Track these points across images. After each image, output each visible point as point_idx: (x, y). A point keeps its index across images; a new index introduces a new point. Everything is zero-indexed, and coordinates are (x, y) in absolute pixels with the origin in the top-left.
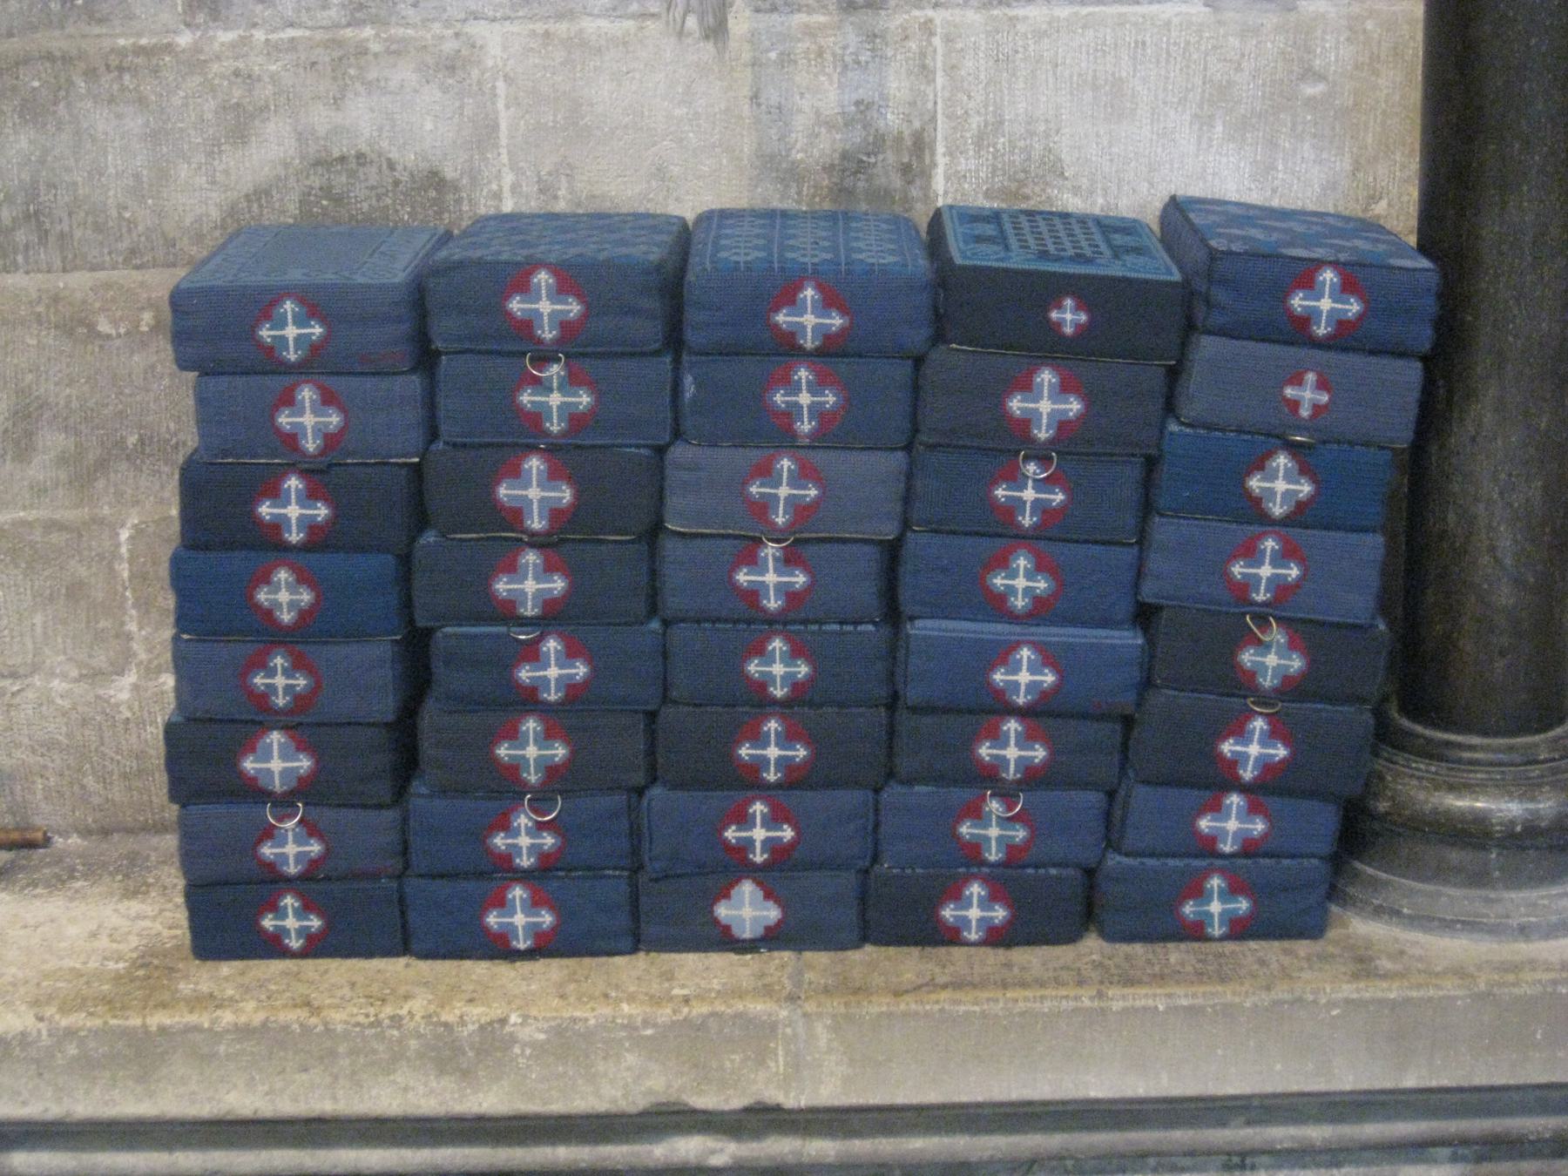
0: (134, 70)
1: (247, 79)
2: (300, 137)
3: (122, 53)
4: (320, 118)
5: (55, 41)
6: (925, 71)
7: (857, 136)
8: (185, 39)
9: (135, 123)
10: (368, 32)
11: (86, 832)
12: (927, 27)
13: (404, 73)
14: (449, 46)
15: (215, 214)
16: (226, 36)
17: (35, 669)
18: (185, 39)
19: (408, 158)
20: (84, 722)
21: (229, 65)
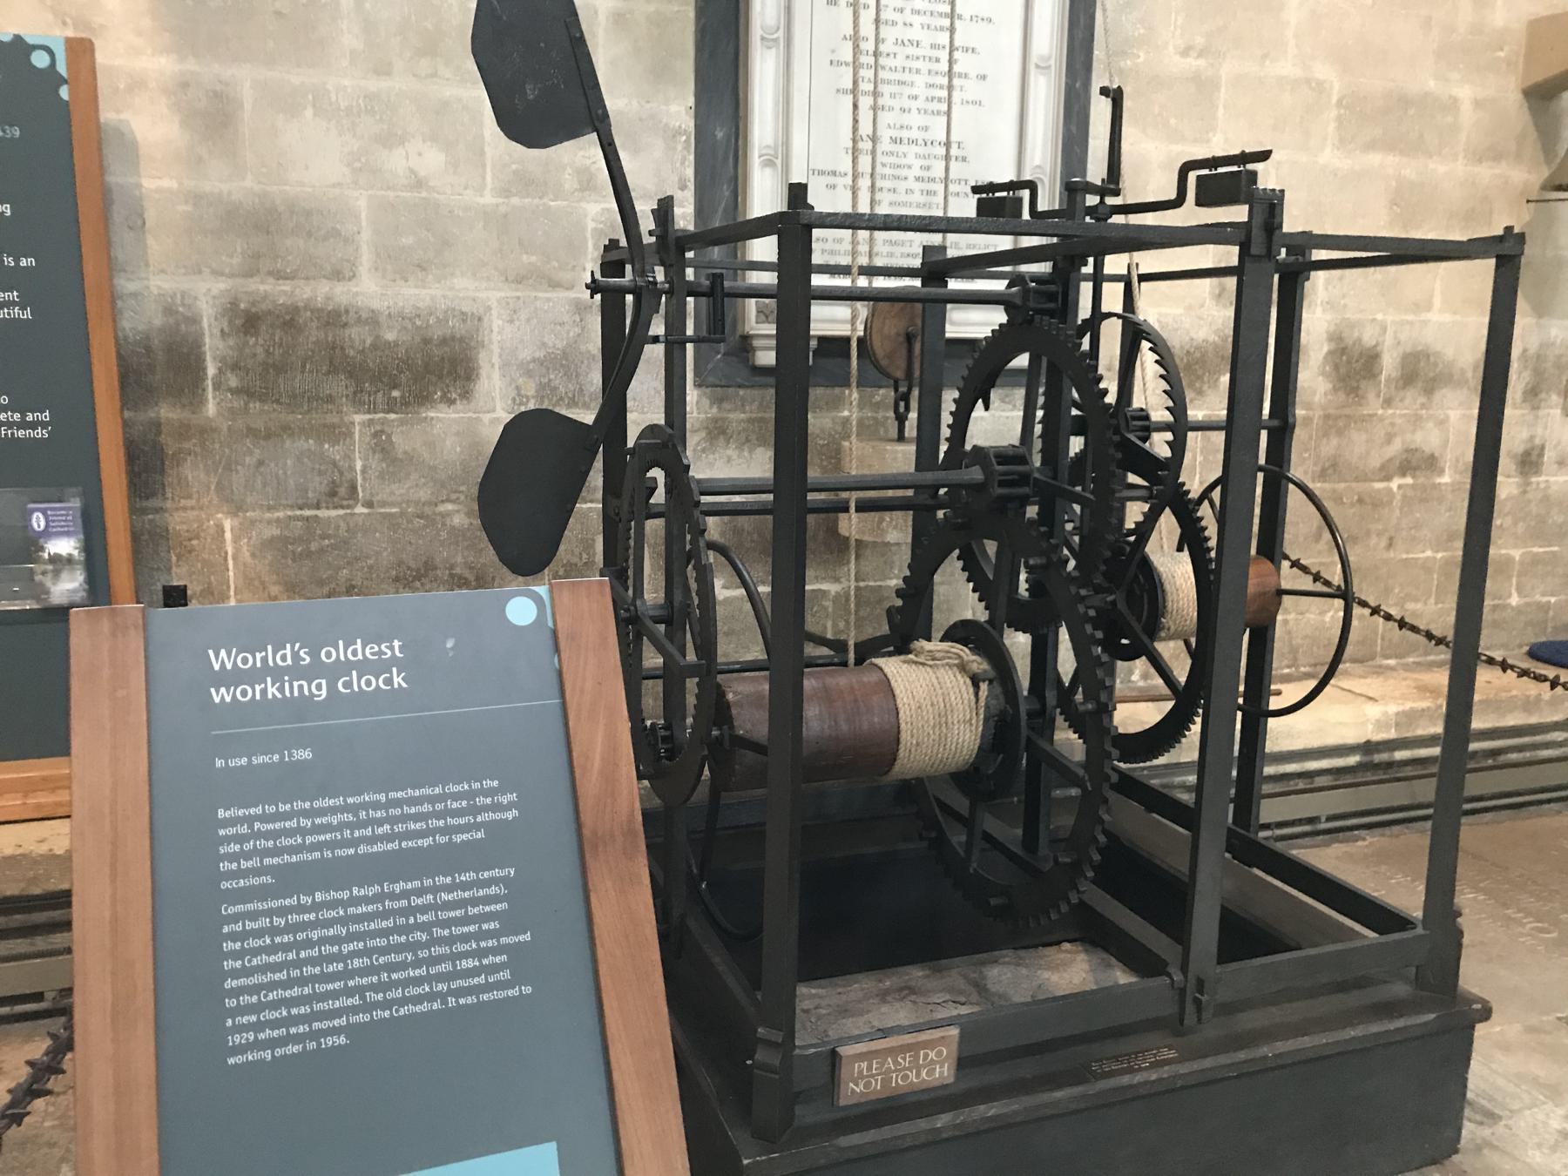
0: (1366, 421)
1: (1393, 424)
2: (1403, 443)
3: (1364, 415)
4: (1409, 436)
5: (1347, 411)
6: (1546, 428)
7: (1529, 445)
8: (1380, 412)
9: (1364, 437)
10: (1424, 412)
11: (1310, 666)
12: (1549, 414)
13: (1430, 425)
14: (1442, 417)
15: (1378, 465)
16: (1390, 411)
17: (1307, 611)
18: (1380, 412)
19: (1427, 450)
20: (1316, 629)
21: (1390, 420)
